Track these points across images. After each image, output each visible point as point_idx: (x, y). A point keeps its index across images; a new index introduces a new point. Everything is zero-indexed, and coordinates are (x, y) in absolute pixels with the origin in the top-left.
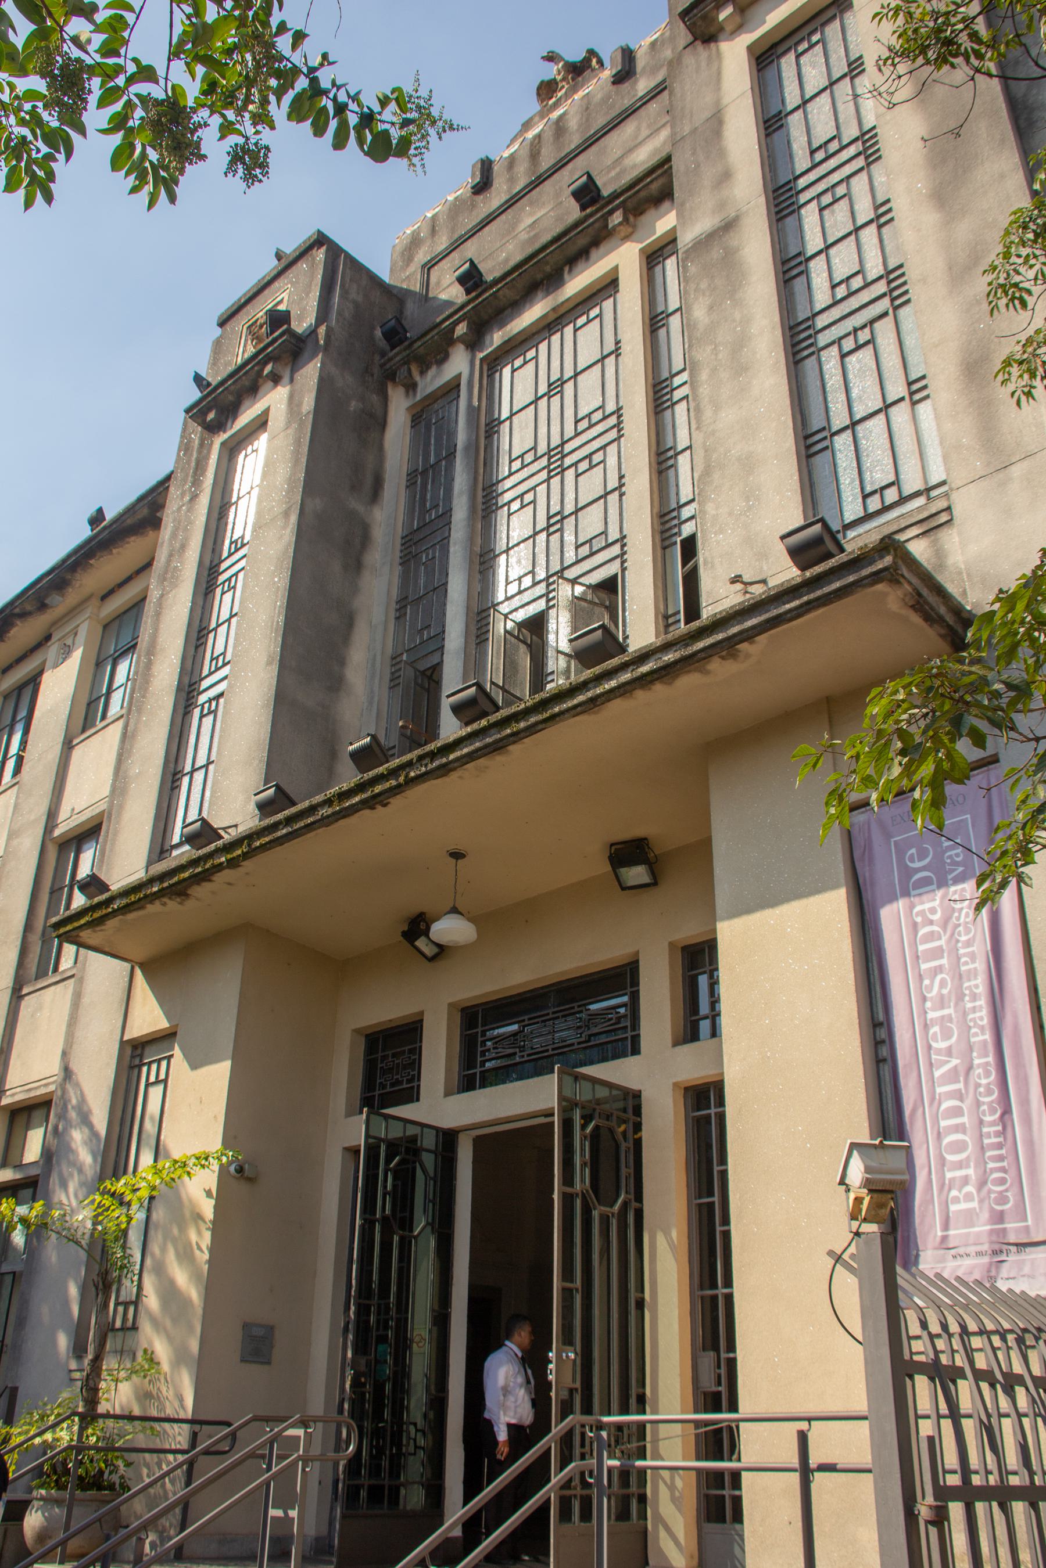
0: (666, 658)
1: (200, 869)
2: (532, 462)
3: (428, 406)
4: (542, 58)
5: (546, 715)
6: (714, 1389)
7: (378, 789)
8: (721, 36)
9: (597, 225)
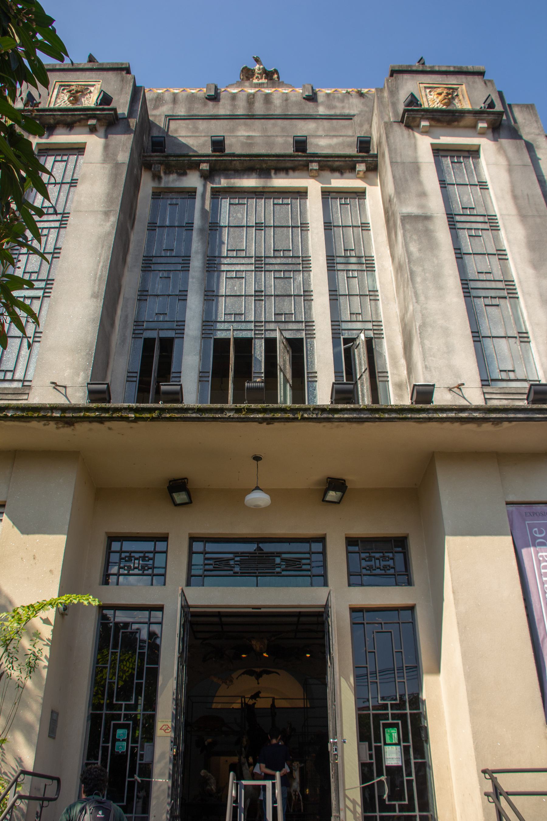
0: (475, 415)
1: (107, 415)
2: (243, 257)
3: (165, 192)
4: (254, 57)
5: (401, 416)
6: (369, 761)
7: (278, 415)
8: (415, 129)
9: (301, 163)
